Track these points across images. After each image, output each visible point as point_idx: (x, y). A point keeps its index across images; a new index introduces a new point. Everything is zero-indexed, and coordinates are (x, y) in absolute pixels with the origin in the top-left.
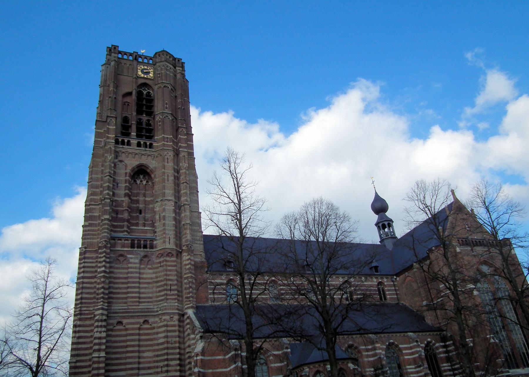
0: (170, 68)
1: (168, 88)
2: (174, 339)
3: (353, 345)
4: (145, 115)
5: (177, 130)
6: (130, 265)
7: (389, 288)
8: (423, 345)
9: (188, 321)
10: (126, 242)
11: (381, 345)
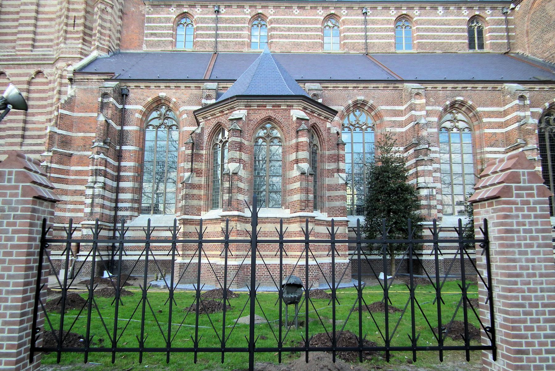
3: (367, 102)
7: (494, 27)
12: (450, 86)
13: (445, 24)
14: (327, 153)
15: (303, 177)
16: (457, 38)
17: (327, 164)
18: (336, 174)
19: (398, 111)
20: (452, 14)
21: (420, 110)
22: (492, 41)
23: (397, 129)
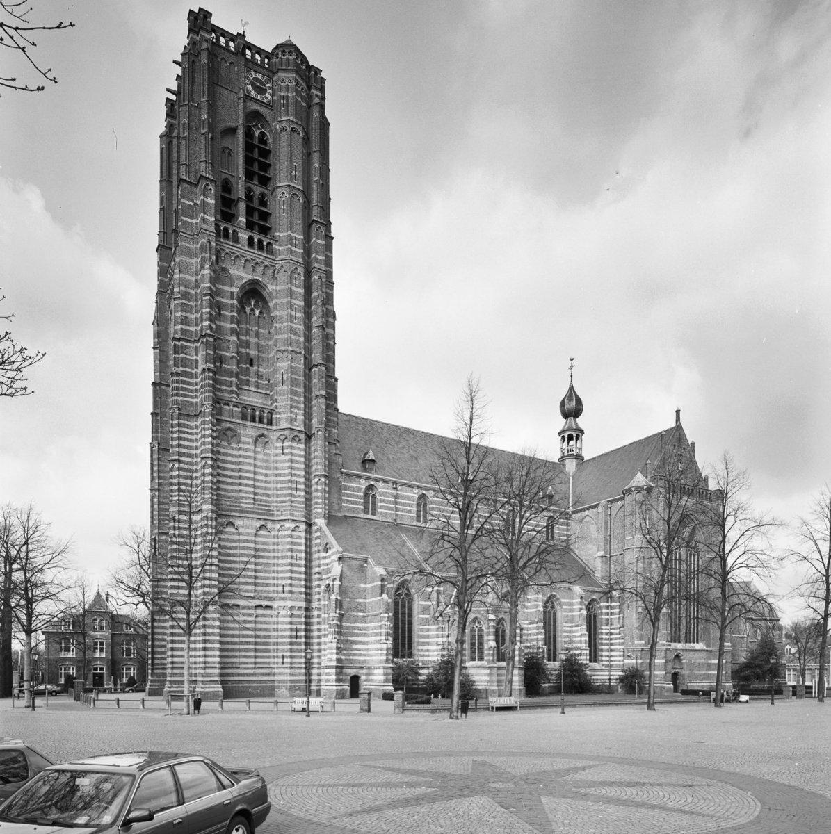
0: (302, 89)
1: (299, 134)
2: (299, 555)
4: (257, 183)
5: (310, 226)
6: (241, 445)
8: (587, 603)
9: (318, 534)
10: (235, 409)
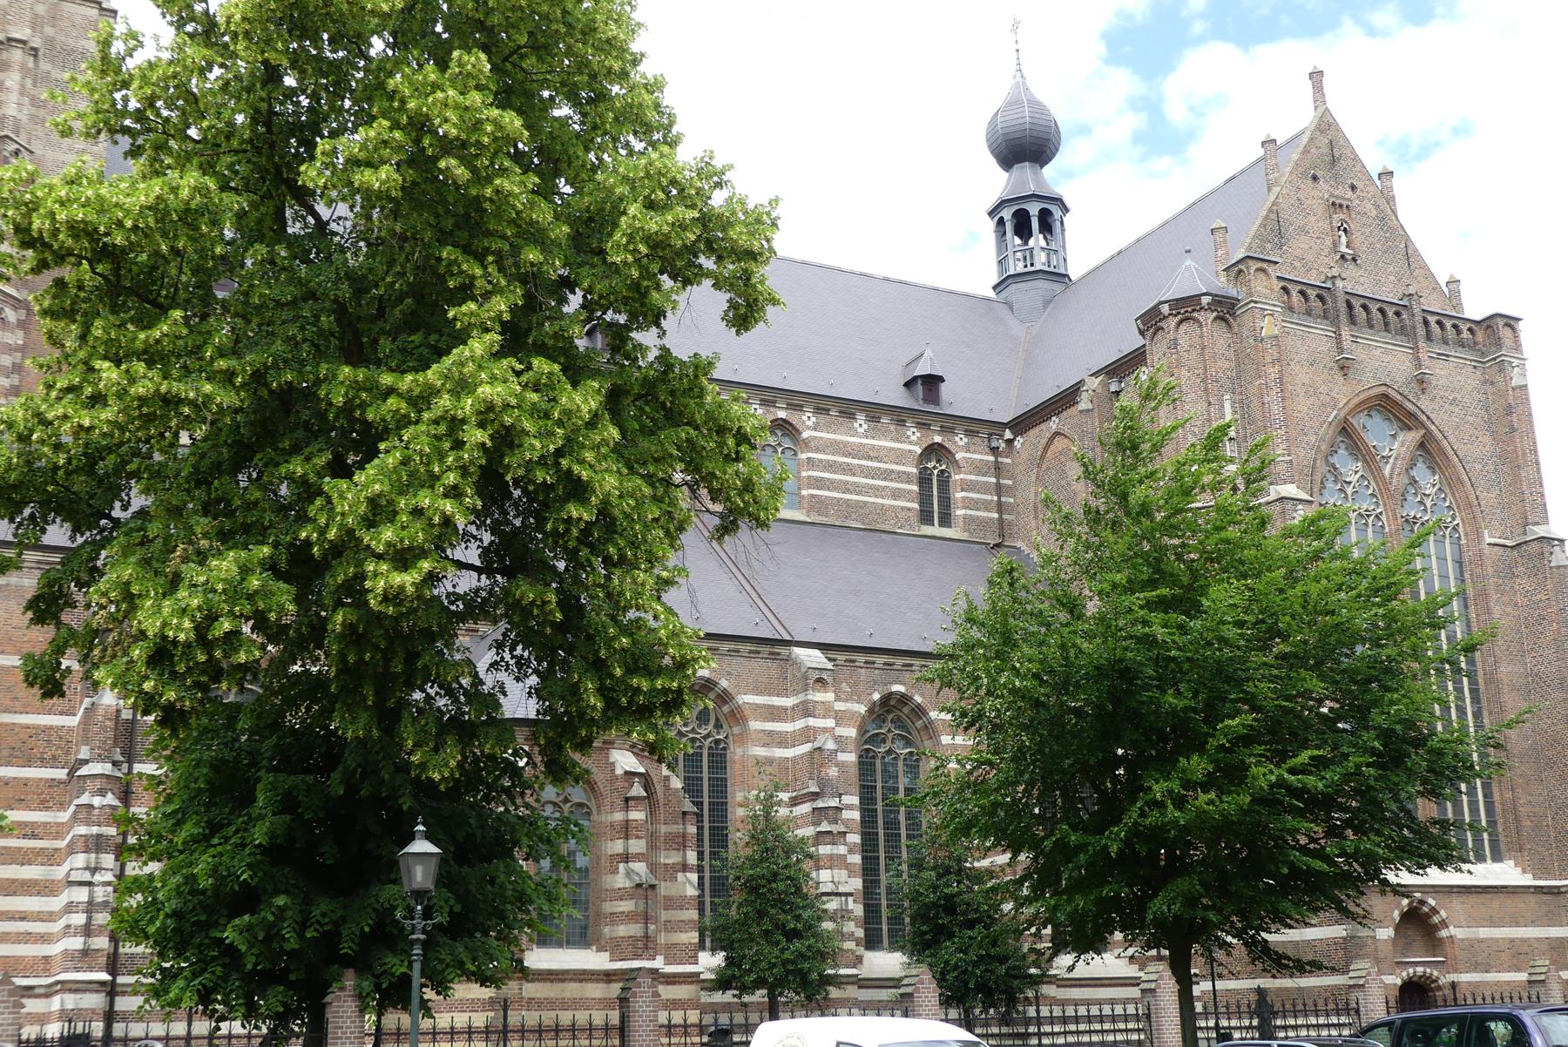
7: (973, 477)
11: (838, 699)
12: (880, 660)
13: (870, 458)
14: (663, 829)
15: (640, 891)
16: (897, 494)
17: (663, 853)
18: (680, 875)
19: (778, 708)
20: (885, 434)
21: (824, 717)
22: (969, 512)
23: (776, 750)
